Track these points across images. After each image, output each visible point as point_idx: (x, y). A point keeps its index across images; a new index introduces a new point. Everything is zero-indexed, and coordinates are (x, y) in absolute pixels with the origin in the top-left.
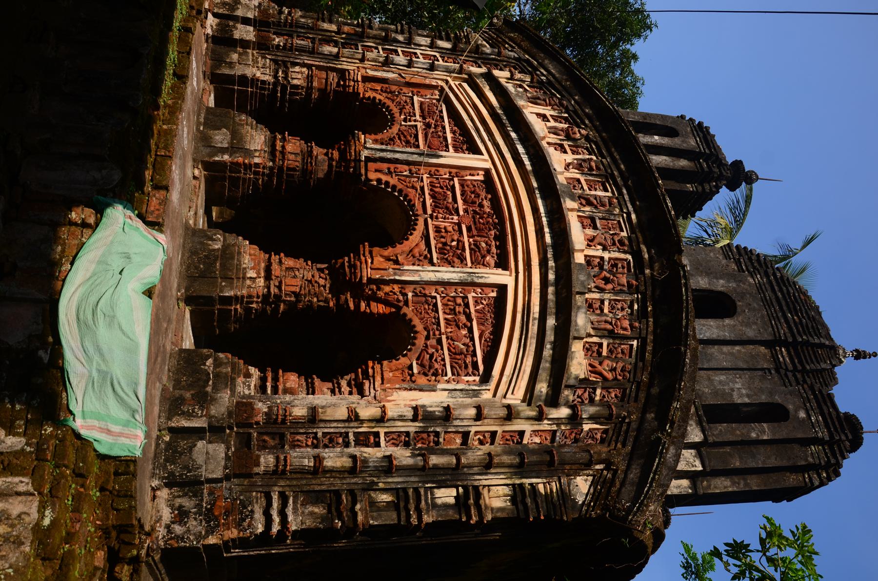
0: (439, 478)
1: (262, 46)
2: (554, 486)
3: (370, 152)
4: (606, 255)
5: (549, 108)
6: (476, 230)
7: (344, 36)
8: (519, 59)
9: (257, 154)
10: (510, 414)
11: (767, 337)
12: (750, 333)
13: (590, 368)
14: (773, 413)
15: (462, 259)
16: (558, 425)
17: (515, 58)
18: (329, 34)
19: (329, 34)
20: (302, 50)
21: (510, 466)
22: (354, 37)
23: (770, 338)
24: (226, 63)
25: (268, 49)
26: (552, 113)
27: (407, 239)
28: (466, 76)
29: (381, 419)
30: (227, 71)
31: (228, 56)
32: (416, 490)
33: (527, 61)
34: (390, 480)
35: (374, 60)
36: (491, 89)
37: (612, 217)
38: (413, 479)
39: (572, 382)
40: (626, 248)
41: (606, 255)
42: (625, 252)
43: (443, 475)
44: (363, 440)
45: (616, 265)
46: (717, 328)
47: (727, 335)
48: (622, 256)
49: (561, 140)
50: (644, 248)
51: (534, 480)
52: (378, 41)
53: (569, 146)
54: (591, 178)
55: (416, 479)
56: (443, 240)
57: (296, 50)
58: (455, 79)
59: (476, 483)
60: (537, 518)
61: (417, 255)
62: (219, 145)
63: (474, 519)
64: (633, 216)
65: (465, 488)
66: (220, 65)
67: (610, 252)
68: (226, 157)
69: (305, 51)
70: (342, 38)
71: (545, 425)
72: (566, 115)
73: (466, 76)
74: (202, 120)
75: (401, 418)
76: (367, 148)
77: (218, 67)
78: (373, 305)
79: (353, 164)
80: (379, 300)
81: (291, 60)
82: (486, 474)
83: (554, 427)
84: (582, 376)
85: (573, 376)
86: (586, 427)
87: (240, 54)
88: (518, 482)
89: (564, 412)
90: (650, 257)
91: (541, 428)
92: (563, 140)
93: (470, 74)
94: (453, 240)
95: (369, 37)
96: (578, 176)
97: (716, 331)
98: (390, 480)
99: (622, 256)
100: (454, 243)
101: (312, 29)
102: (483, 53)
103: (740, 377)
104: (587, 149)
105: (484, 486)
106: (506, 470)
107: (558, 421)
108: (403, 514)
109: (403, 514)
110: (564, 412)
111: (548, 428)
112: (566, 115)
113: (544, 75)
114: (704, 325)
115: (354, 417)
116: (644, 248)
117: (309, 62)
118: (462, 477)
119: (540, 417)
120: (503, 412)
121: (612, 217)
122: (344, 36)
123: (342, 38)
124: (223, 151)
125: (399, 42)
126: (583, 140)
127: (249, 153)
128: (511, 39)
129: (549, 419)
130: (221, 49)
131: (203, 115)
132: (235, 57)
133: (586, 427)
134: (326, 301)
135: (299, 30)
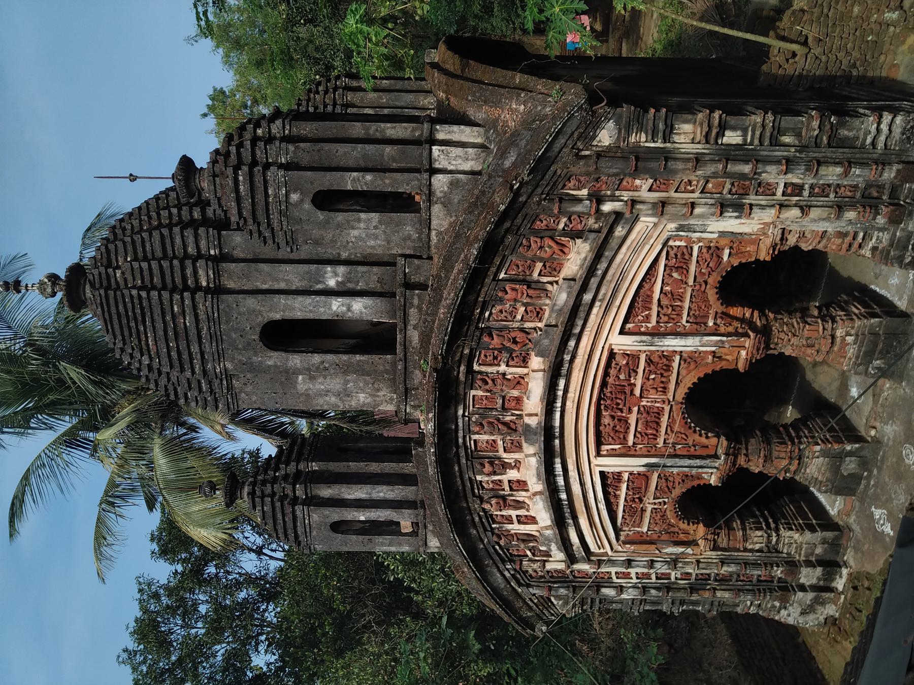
0: (741, 153)
1: (792, 565)
2: (633, 139)
3: (713, 464)
4: (503, 368)
5: (513, 532)
6: (625, 390)
7: (708, 587)
8: (528, 586)
9: (817, 454)
10: (661, 207)
11: (230, 298)
12: (251, 302)
13: (566, 250)
14: (327, 200)
15: (649, 361)
16: (613, 195)
17: (532, 586)
18: (723, 587)
19: (723, 587)
20: (755, 565)
21: (676, 159)
22: (698, 587)
23: (224, 297)
24: (828, 543)
25: (786, 562)
26: (510, 527)
27: (699, 379)
28: (592, 558)
29: (782, 206)
30: (829, 535)
31: (825, 551)
32: (761, 144)
33: (520, 585)
34: (786, 153)
35: (687, 563)
36: (572, 545)
37: (481, 411)
38: (765, 153)
39: (592, 236)
40: (479, 377)
41: (503, 368)
42: (480, 373)
43: (737, 155)
44: (798, 189)
45: (495, 358)
46: (294, 309)
47: (282, 300)
48: (484, 369)
49: (512, 495)
50: (462, 377)
51: (652, 145)
52: (675, 586)
53: (503, 490)
54: (491, 454)
55: (762, 153)
56: (664, 380)
57: (760, 564)
58: (606, 554)
59: (708, 146)
60: (658, 110)
61: (692, 363)
62: (853, 459)
63: (716, 115)
64: (460, 412)
65: (717, 143)
66: (833, 540)
67: (498, 372)
68: (848, 448)
69: (753, 564)
70: (709, 584)
71: (626, 195)
72: (493, 526)
73: (592, 558)
74: (863, 482)
75: (762, 207)
76: (715, 468)
77: (837, 538)
78: (740, 315)
79: (731, 450)
80: (737, 319)
81: (764, 555)
82: (697, 153)
83: (617, 193)
84: (579, 241)
85: (589, 241)
86: (584, 192)
87: (812, 554)
88: (668, 145)
89: (607, 207)
90: (459, 367)
91: (631, 193)
92: (509, 495)
93: (589, 561)
94: (654, 379)
95: (685, 589)
96: (505, 455)
97: (297, 305)
98: (786, 153)
99: (484, 369)
100: (652, 376)
101: (739, 590)
102: (568, 587)
103: (348, 242)
104: (483, 488)
105: (699, 143)
106: (679, 156)
107: (614, 198)
108: (777, 124)
109: (777, 124)
110: (607, 207)
111: (625, 193)
112: (493, 526)
113: (507, 570)
114: (311, 311)
115: (805, 209)
116: (462, 377)
117: (747, 554)
118: (721, 152)
119: (633, 202)
120: (669, 209)
121: (481, 411)
122: (708, 587)
123: (709, 584)
124: (850, 454)
125: (654, 588)
126: (486, 497)
127: (824, 454)
128: (530, 608)
129: (622, 201)
130: (830, 557)
131: (862, 486)
132: (819, 550)
133: (584, 192)
134: (776, 319)
135: (750, 588)
